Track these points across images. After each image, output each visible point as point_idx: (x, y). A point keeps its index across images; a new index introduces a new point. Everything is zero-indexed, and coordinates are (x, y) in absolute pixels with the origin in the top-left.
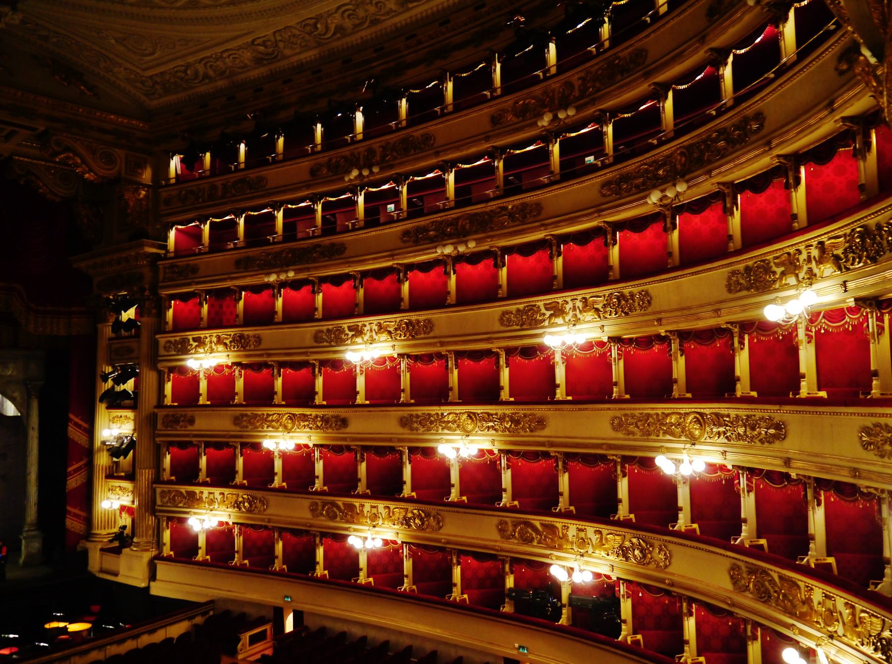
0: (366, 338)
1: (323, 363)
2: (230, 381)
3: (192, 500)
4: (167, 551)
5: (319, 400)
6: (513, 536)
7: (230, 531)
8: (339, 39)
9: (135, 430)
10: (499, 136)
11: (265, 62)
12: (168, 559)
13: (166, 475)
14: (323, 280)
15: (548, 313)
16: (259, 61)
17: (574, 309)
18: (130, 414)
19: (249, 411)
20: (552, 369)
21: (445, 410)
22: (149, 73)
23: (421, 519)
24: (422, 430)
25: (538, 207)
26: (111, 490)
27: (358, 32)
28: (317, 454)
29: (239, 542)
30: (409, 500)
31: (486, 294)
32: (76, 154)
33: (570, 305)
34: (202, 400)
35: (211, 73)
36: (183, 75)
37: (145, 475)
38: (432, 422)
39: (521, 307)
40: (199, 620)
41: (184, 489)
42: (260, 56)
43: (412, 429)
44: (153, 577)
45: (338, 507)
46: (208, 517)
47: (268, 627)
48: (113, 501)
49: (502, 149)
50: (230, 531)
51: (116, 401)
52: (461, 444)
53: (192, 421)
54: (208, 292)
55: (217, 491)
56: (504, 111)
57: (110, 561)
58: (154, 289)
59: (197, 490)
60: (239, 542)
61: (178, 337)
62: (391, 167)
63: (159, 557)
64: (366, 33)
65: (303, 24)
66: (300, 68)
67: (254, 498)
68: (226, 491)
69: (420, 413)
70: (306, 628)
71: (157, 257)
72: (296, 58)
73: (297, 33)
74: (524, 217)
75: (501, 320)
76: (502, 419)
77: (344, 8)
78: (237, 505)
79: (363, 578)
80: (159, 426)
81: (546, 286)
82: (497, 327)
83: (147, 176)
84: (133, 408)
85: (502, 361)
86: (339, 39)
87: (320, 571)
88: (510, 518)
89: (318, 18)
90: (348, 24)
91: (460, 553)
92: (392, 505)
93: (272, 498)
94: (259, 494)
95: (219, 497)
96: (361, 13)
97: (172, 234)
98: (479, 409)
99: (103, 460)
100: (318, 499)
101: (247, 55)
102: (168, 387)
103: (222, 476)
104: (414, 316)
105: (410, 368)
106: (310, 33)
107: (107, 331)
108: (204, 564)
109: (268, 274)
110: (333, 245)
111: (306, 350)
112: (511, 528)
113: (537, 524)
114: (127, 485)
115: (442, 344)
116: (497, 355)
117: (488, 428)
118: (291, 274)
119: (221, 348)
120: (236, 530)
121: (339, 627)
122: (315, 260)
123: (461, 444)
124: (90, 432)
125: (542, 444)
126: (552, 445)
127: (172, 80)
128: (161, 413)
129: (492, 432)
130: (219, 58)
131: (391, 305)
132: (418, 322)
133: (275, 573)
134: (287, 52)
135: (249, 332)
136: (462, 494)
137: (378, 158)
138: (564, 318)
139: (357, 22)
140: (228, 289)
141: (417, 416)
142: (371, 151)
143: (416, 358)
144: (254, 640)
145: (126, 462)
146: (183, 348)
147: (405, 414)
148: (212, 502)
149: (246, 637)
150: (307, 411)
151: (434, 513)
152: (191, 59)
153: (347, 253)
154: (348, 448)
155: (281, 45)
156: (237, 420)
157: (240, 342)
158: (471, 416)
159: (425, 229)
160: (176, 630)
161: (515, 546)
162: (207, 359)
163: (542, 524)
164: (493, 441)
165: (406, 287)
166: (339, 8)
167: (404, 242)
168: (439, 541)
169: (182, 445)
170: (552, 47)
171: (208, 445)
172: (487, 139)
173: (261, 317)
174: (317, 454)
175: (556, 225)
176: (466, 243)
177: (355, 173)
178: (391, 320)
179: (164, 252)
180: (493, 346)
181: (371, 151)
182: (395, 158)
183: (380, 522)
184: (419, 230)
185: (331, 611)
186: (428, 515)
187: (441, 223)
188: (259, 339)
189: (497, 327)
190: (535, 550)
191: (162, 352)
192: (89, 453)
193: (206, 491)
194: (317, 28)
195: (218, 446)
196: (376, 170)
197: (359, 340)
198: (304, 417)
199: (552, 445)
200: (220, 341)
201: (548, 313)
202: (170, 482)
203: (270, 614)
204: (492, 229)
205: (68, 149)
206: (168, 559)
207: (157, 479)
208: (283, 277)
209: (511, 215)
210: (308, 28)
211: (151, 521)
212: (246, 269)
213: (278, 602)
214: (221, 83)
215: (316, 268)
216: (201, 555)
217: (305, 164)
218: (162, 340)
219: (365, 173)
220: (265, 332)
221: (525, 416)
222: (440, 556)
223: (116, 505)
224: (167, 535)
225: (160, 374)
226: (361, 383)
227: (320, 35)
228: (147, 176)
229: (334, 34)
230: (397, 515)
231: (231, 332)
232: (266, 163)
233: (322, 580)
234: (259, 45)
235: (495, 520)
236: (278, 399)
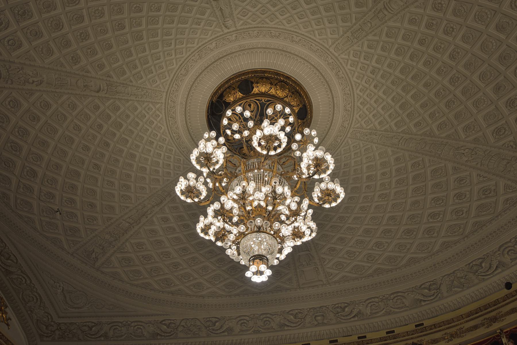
8: (225, 336)
11: (159, 337)
27: (242, 335)
36: (86, 328)
42: (159, 332)
73: (198, 323)
77: (242, 318)
86: (225, 336)
106: (206, 327)
127: (75, 331)
155: (180, 329)
166: (239, 317)
194: (215, 325)
210: (208, 323)
227: (213, 330)
229: (223, 332)
234: (165, 324)
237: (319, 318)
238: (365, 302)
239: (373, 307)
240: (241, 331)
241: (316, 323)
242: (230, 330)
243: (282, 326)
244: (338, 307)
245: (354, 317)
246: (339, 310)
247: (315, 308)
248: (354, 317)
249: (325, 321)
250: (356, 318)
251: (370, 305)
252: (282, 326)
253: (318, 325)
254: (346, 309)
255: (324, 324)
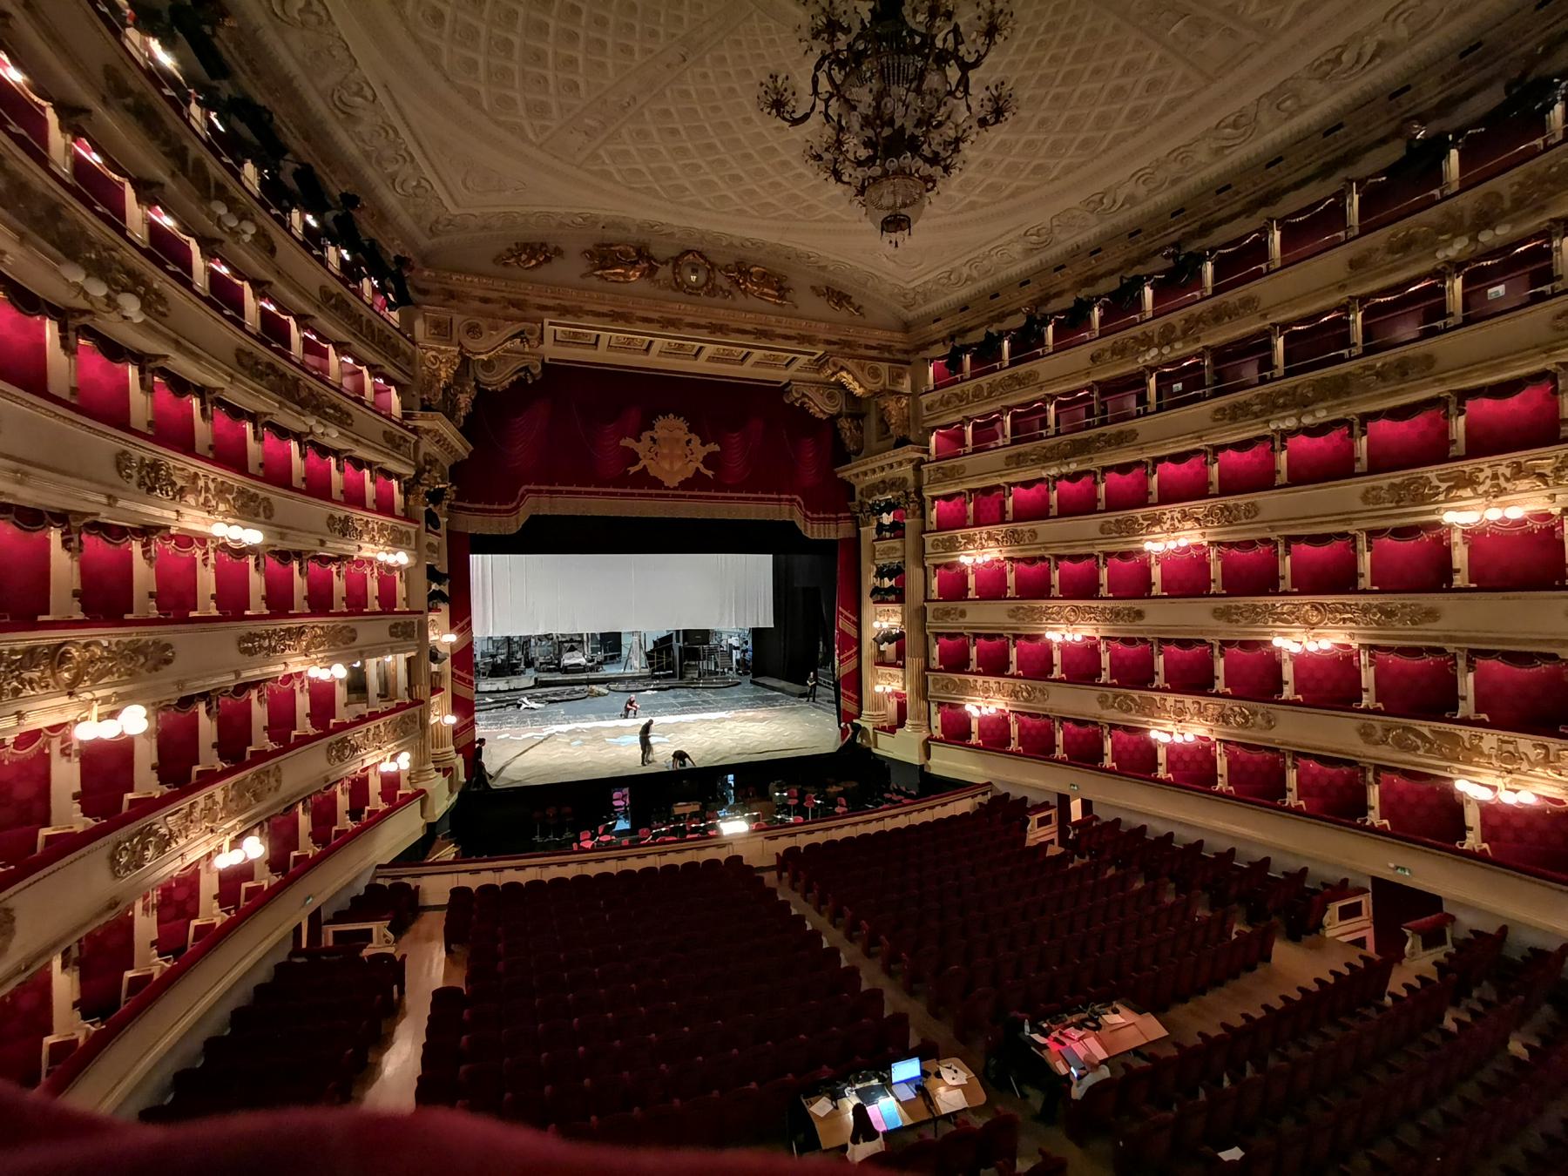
0: (1165, 527)
1: (1108, 555)
2: (1002, 574)
3: (965, 688)
4: (938, 733)
5: (1103, 592)
6: (1385, 742)
7: (1005, 719)
9: (903, 622)
10: (1360, 283)
12: (940, 740)
13: (935, 664)
14: (1105, 470)
15: (1444, 486)
16: (1028, 252)
17: (1495, 477)
18: (897, 607)
19: (1026, 604)
20: (1448, 551)
21: (1277, 601)
22: (912, 285)
23: (1245, 717)
24: (1244, 622)
25: (1429, 360)
26: (883, 676)
28: (1103, 647)
29: (1014, 730)
30: (1224, 696)
31: (1338, 468)
32: (849, 372)
33: (1488, 472)
34: (971, 594)
35: (975, 273)
37: (913, 663)
38: (1257, 614)
39: (1397, 481)
40: (980, 799)
41: (956, 677)
43: (1230, 621)
44: (928, 756)
45: (1133, 700)
46: (985, 703)
47: (1052, 812)
48: (885, 685)
49: (1363, 299)
50: (1005, 719)
51: (880, 595)
52: (1303, 638)
53: (963, 614)
54: (971, 491)
55: (992, 680)
56: (1371, 251)
57: (883, 738)
58: (919, 492)
59: (971, 678)
60: (1014, 730)
61: (946, 535)
62: (1198, 340)
63: (931, 738)
64: (1160, 198)
65: (1088, 202)
66: (1074, 253)
67: (1034, 689)
68: (1002, 680)
69: (1241, 604)
70: (1097, 818)
71: (921, 461)
72: (1072, 242)
73: (1077, 213)
74: (1405, 374)
75: (1365, 498)
76: (1365, 610)
78: (1014, 694)
79: (1162, 772)
80: (929, 618)
81: (1436, 451)
82: (1359, 505)
83: (906, 385)
84: (900, 599)
85: (1362, 544)
87: (1108, 762)
88: (1378, 722)
89: (1104, 194)
90: (1142, 190)
91: (1297, 755)
92: (1203, 701)
93: (1053, 689)
94: (1039, 684)
95: (995, 686)
96: (1160, 175)
97: (933, 439)
98: (1329, 600)
99: (868, 650)
100: (1109, 692)
101: (1018, 247)
102: (935, 583)
103: (995, 665)
104: (1230, 501)
105: (1220, 555)
107: (868, 532)
108: (977, 747)
109: (1049, 468)
110: (1121, 432)
111: (1091, 541)
112: (1379, 733)
113: (1426, 731)
114: (897, 672)
115: (1273, 529)
116: (1354, 537)
117: (1344, 620)
118: (1073, 467)
119: (992, 543)
120: (1012, 718)
121: (1137, 822)
122: (1098, 450)
123: (1303, 638)
124: (858, 625)
125: (1436, 639)
126: (1451, 639)
128: (930, 607)
129: (1349, 624)
130: (988, 256)
131: (1198, 491)
132: (1237, 506)
133: (1057, 761)
134: (1062, 237)
135: (1023, 527)
136: (1297, 693)
137: (1178, 332)
138: (1474, 490)
139: (1152, 186)
140: (998, 487)
141: (1237, 608)
142: (1169, 328)
143: (1231, 545)
144: (1043, 822)
145: (897, 650)
146: (952, 545)
147: (1221, 606)
148: (987, 690)
149: (1034, 819)
150: (1094, 603)
151: (1262, 710)
152: (957, 263)
153: (1139, 439)
154: (1144, 640)
155: (1057, 230)
156: (1013, 613)
157: (1014, 538)
158: (1314, 607)
159: (1247, 404)
160: (962, 806)
161: (1388, 754)
162: (980, 554)
163: (1433, 732)
164: (1352, 636)
165: (1215, 470)
167: (1216, 420)
168: (1272, 741)
169: (950, 636)
170: (1454, 153)
171: (977, 636)
172: (1343, 287)
173: (1038, 512)
174: (1103, 647)
175: (1462, 377)
176: (1313, 413)
177: (1154, 352)
178: (1199, 507)
179: (925, 456)
180: (1351, 529)
181: (1169, 328)
182: (1202, 330)
183: (1188, 717)
184: (1235, 407)
185: (1123, 802)
186: (1254, 714)
187: (1269, 395)
188: (1034, 533)
189: (1359, 505)
190: (1423, 760)
191: (929, 549)
192: (859, 642)
193: (980, 679)
195: (989, 637)
196: (1178, 345)
197: (1157, 529)
198: (1090, 610)
199: (1451, 639)
200: (990, 537)
201: (1444, 486)
202: (939, 670)
203: (1054, 801)
204: (1348, 394)
205: (842, 369)
206: (940, 740)
207: (927, 668)
208: (1064, 470)
209: (1381, 375)
211: (924, 705)
212: (1018, 465)
213: (1065, 790)
214: (984, 284)
215: (1101, 458)
216: (974, 739)
217: (1085, 351)
218: (929, 539)
219: (1166, 350)
220: (1040, 526)
221: (1404, 606)
222: (1268, 755)
223: (889, 689)
224: (937, 720)
225: (925, 569)
226: (1156, 573)
228: (906, 385)
230: (1210, 712)
231: (1004, 527)
232: (1037, 356)
233: (1110, 771)
235: (1356, 723)
236: (1055, 592)
237: (1288, 103)
238: (1385, 19)
239: (1411, 20)
240: (1149, 191)
241: (1285, 115)
242: (1131, 200)
243: (1218, 152)
244: (1321, 65)
245: (1369, 62)
246: (1327, 68)
247: (1267, 94)
248: (1369, 62)
249: (1305, 102)
250: (1378, 61)
251: (1401, 19)
252: (1218, 152)
253: (1291, 115)
254: (1344, 57)
255: (1303, 108)
